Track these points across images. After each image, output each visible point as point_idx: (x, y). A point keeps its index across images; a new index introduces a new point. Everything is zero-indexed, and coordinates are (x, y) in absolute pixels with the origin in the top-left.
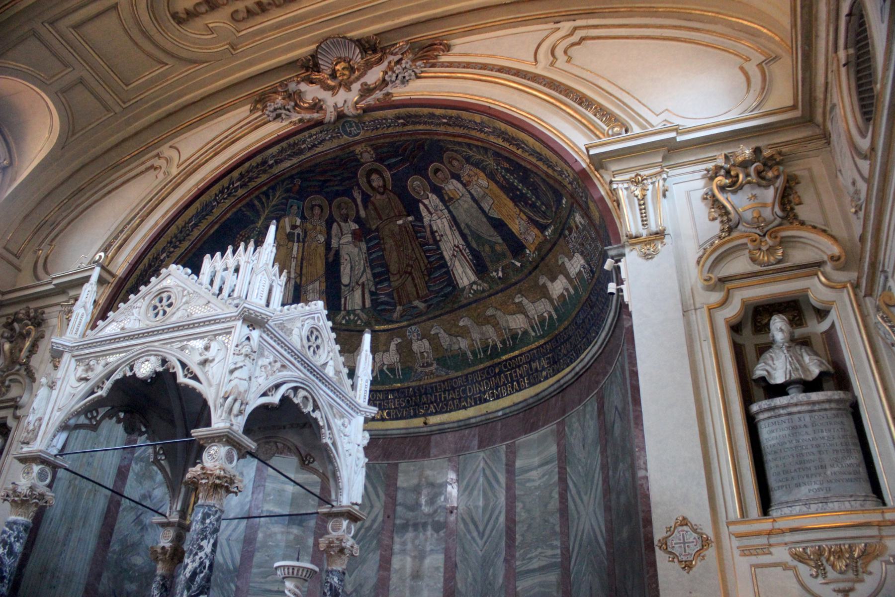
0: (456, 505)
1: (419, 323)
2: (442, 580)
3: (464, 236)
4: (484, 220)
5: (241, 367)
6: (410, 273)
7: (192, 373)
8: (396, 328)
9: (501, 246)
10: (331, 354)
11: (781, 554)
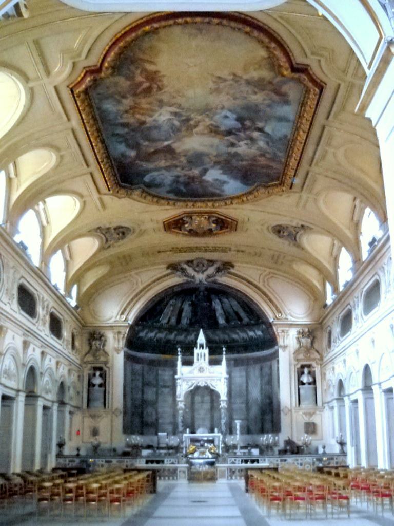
3: (224, 311)
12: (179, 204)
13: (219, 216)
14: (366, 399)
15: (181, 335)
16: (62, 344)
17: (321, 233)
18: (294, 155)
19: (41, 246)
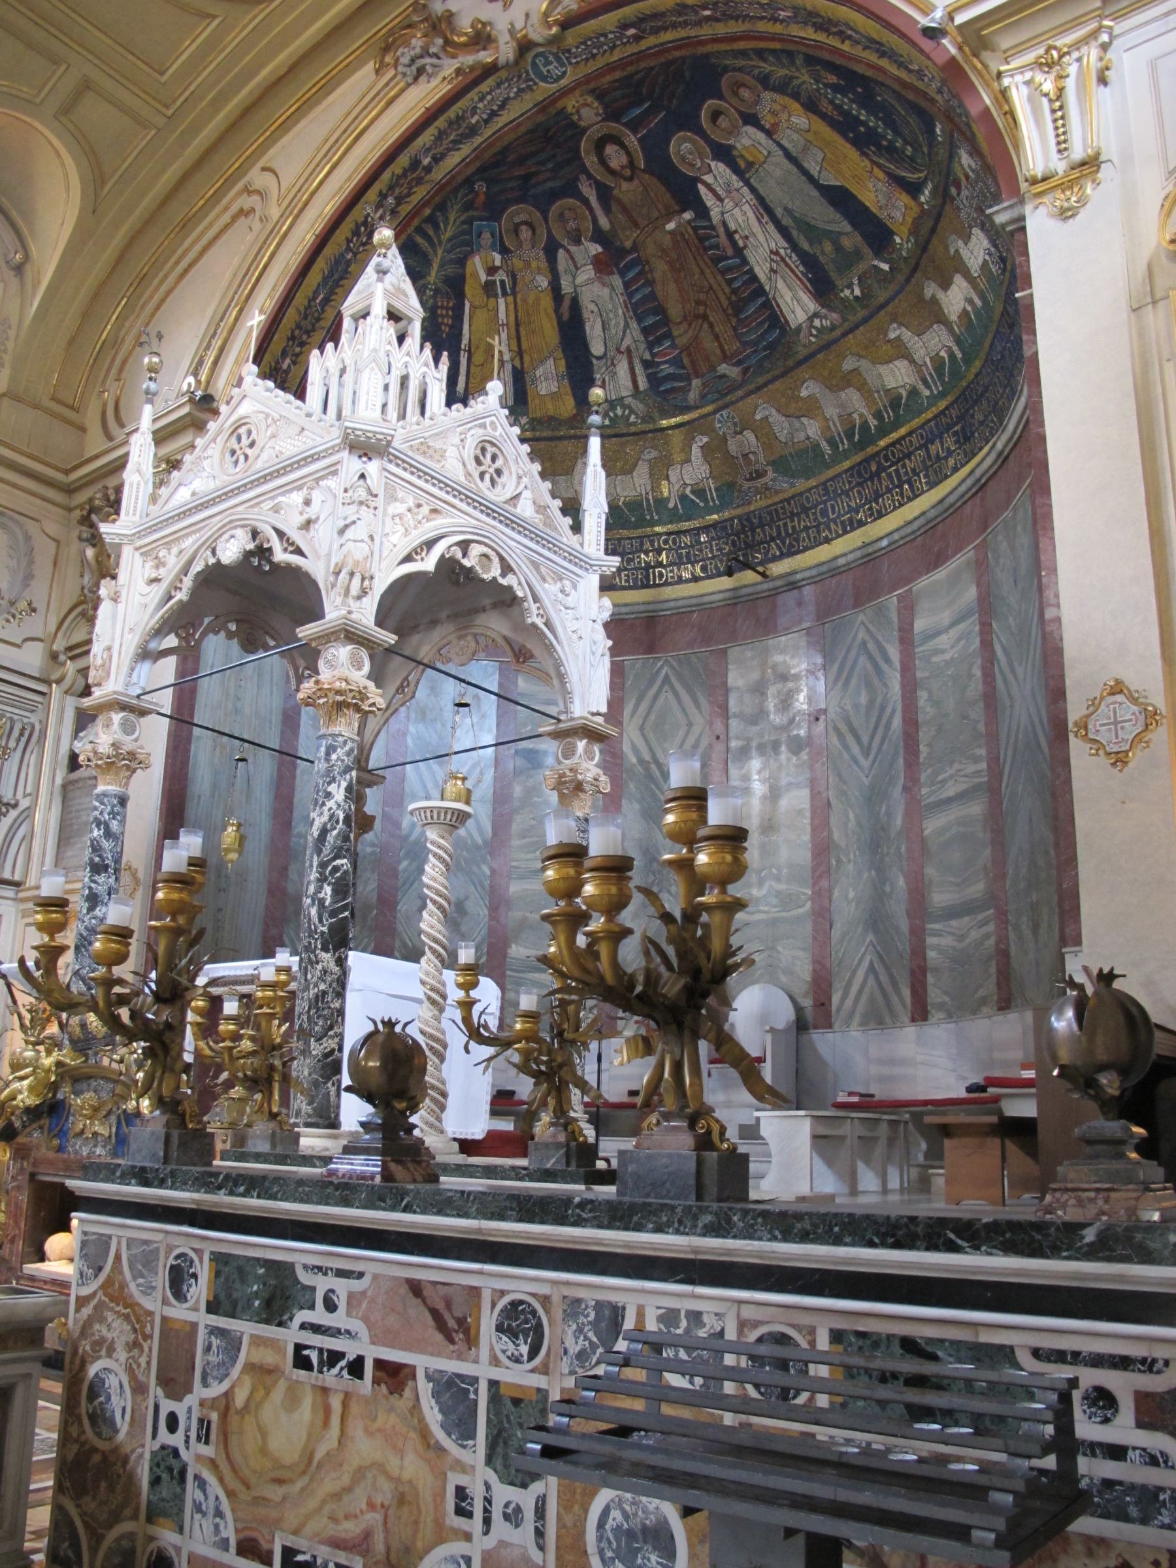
0: (823, 706)
1: (733, 403)
2: (809, 829)
3: (784, 232)
4: (815, 193)
5: (354, 522)
6: (705, 317)
7: (293, 544)
8: (697, 419)
9: (852, 240)
10: (525, 480)
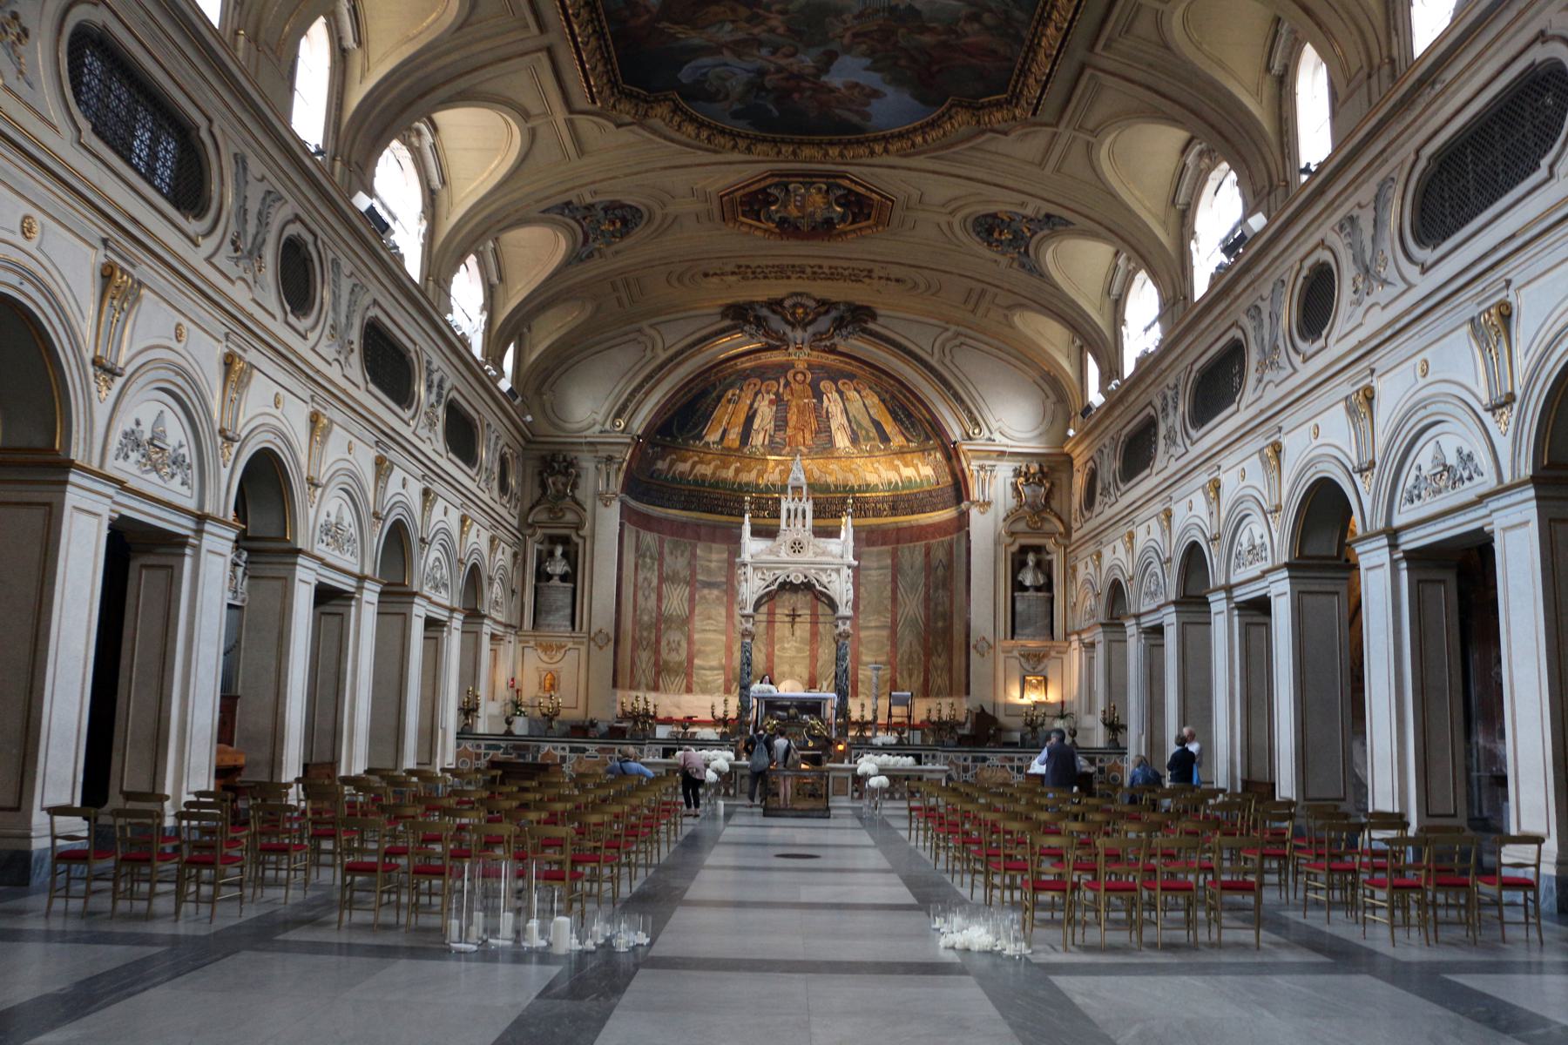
3: (849, 421)
9: (873, 432)
11: (1016, 653)
12: (760, 147)
13: (853, 187)
14: (1183, 628)
15: (749, 471)
16: (477, 479)
17: (1094, 236)
18: (1055, 15)
19: (424, 237)
